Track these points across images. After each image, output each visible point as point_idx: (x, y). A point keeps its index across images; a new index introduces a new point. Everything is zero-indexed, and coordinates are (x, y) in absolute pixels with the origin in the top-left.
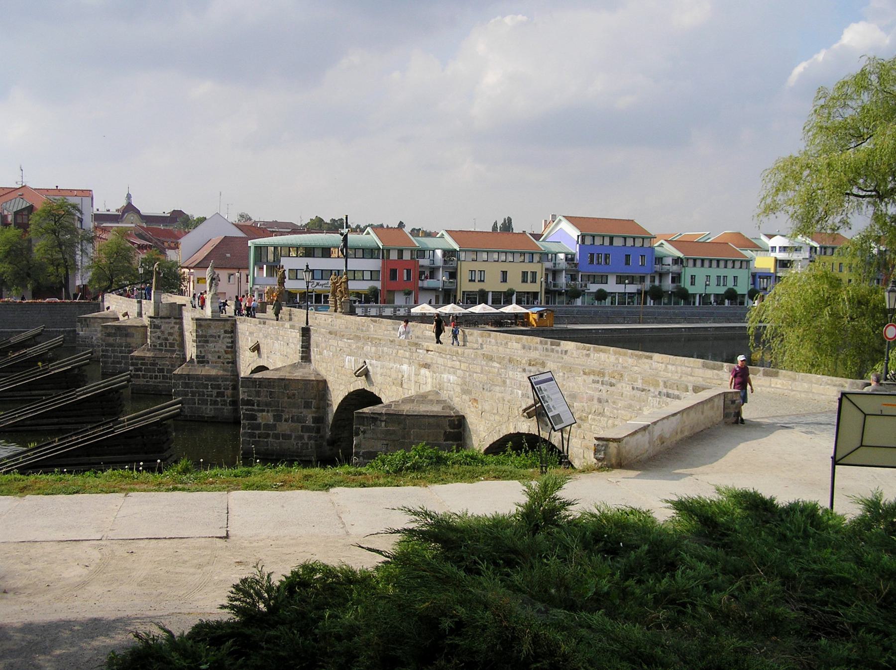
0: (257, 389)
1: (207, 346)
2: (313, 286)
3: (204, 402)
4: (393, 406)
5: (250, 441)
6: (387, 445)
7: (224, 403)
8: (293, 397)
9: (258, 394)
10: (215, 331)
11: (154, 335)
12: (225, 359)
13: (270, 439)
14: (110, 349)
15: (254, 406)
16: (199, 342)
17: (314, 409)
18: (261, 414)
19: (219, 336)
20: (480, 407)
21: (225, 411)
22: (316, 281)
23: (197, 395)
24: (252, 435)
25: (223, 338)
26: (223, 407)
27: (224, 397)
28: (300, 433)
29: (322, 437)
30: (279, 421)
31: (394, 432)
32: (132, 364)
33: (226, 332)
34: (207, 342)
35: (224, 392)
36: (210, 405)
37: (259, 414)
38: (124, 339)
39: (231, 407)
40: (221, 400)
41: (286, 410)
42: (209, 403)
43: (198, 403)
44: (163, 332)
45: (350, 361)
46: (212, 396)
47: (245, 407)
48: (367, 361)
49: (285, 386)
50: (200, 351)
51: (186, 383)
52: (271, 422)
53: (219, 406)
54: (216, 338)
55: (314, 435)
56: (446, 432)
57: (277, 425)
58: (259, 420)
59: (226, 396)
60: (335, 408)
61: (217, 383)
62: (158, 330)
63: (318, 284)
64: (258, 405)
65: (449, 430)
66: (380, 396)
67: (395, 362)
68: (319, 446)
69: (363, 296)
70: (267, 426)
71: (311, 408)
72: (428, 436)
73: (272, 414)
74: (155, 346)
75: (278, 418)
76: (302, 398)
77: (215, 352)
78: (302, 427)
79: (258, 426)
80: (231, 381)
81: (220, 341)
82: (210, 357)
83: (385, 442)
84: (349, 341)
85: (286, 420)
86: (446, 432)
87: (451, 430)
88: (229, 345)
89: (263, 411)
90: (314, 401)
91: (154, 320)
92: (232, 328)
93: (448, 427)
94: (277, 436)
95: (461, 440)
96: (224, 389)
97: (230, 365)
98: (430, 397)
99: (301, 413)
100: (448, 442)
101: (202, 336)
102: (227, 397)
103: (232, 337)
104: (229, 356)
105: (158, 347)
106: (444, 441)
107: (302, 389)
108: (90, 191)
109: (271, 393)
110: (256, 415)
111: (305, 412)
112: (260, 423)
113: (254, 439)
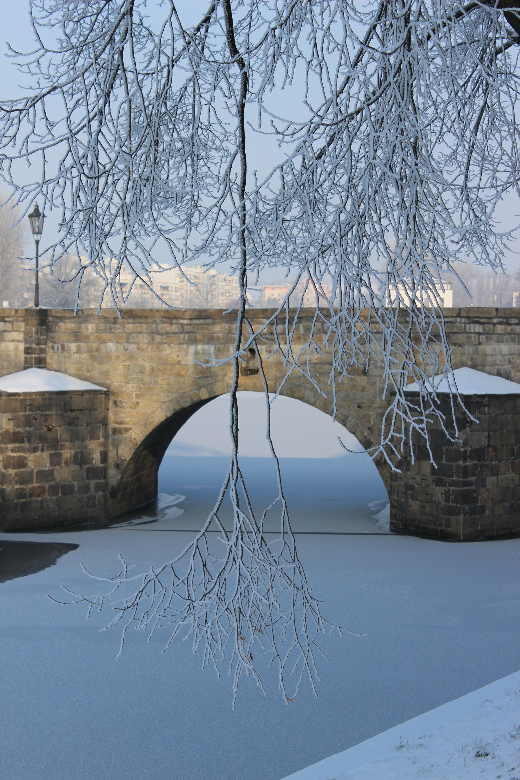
5: (17, 504)
13: (46, 496)
15: (23, 442)
18: (32, 455)
52: (48, 467)
57: (55, 472)
64: (29, 442)
113: (23, 500)
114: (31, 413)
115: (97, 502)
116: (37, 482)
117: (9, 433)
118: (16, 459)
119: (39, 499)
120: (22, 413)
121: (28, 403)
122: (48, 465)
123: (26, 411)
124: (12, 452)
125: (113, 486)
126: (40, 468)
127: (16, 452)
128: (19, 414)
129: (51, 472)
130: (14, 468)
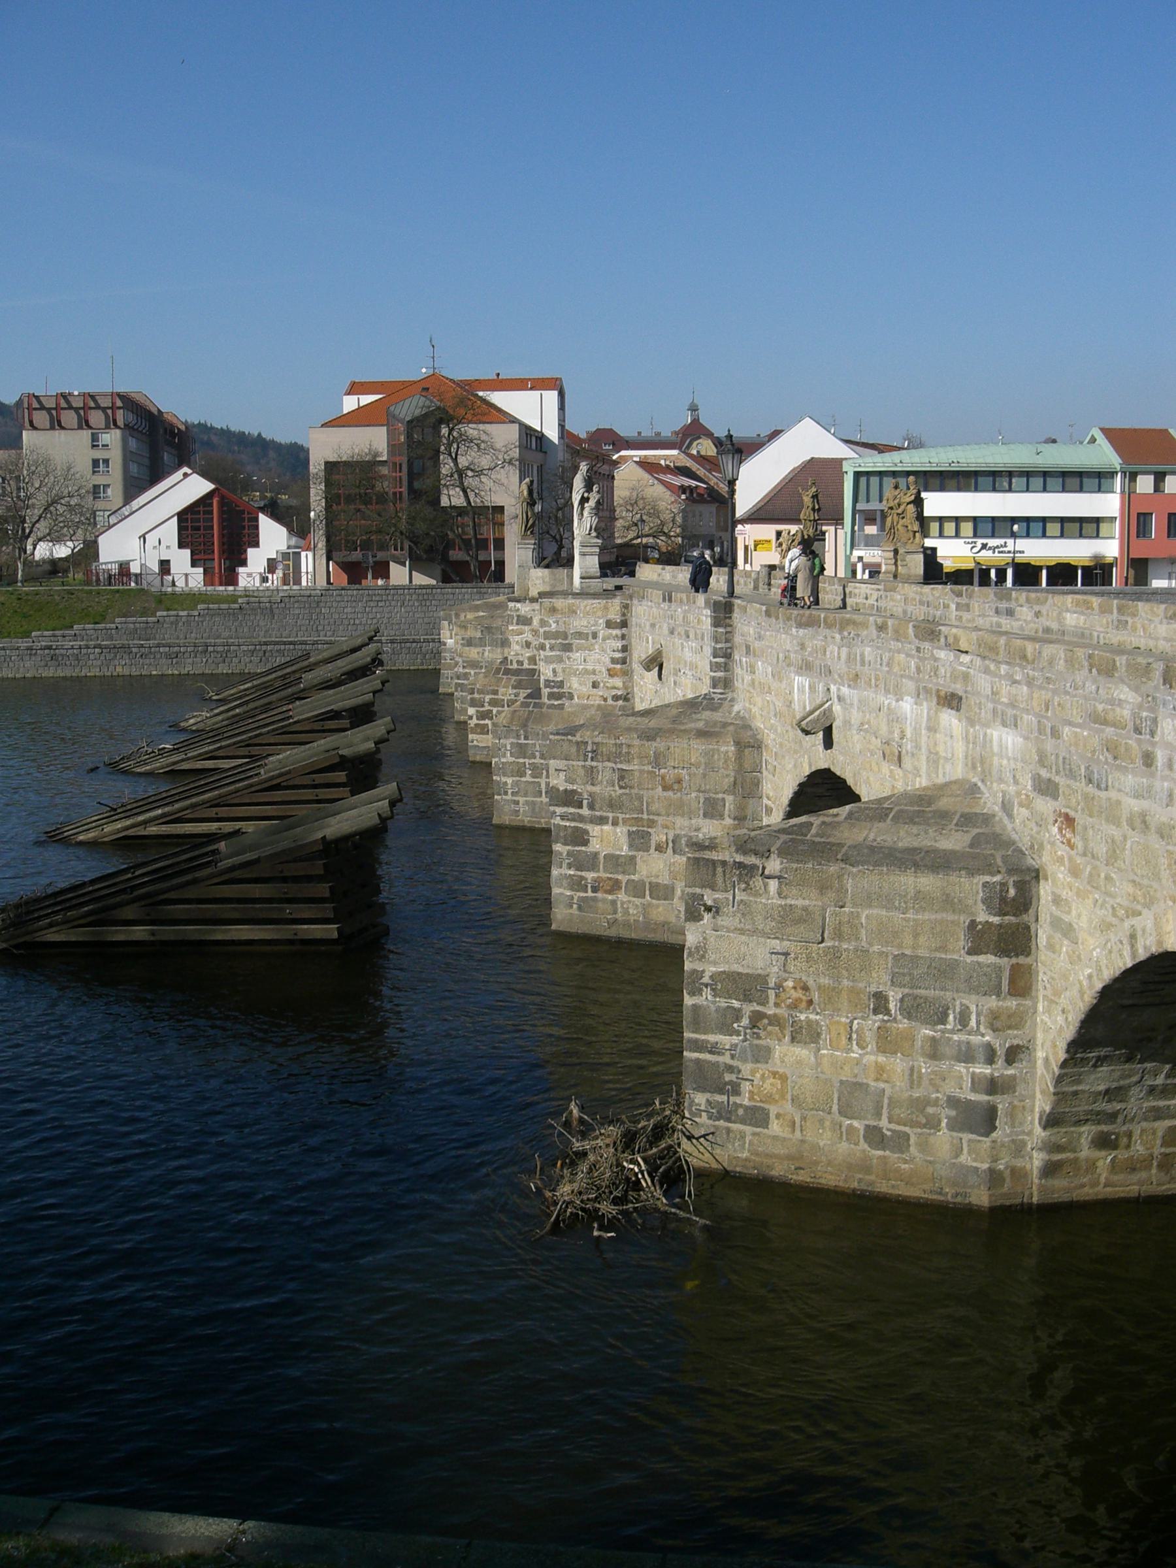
1: (569, 658)
2: (975, 550)
4: (813, 831)
5: (572, 897)
6: (786, 954)
8: (676, 786)
9: (591, 774)
10: (586, 624)
11: (517, 638)
13: (622, 896)
14: (472, 672)
15: (580, 806)
16: (552, 648)
17: (728, 821)
18: (597, 828)
19: (595, 635)
20: (1080, 845)
22: (980, 542)
24: (578, 884)
25: (604, 640)
31: (803, 917)
32: (473, 703)
33: (609, 624)
34: (567, 648)
37: (594, 830)
38: (499, 650)
41: (660, 820)
44: (535, 632)
45: (801, 690)
47: (559, 810)
48: (833, 688)
49: (657, 755)
50: (554, 671)
52: (625, 850)
54: (587, 639)
56: (973, 924)
57: (638, 860)
58: (595, 846)
62: (526, 628)
63: (984, 546)
64: (591, 807)
65: (983, 916)
67: (887, 691)
69: (1080, 572)
70: (614, 861)
71: (722, 817)
72: (916, 936)
73: (625, 829)
74: (520, 663)
75: (640, 840)
76: (699, 791)
77: (586, 672)
79: (591, 862)
81: (597, 647)
82: (575, 685)
83: (776, 944)
85: (659, 848)
86: (973, 924)
87: (996, 920)
88: (618, 655)
89: (602, 821)
90: (729, 799)
91: (518, 605)
92: (624, 615)
93: (981, 906)
94: (637, 889)
95: (1028, 954)
97: (620, 703)
98: (944, 803)
99: (698, 830)
100: (981, 958)
101: (556, 635)
103: (623, 637)
104: (618, 682)
105: (526, 666)
106: (969, 953)
107: (697, 765)
108: (557, 379)
109: (622, 775)
110: (586, 832)
112: (596, 855)
114: (594, 764)
116: (605, 871)
118: (570, 830)
119: (610, 897)
121: (589, 749)
123: (585, 760)
124: (563, 819)
126: (612, 851)
127: (568, 820)
128: (574, 763)
129: (632, 859)
130: (565, 844)
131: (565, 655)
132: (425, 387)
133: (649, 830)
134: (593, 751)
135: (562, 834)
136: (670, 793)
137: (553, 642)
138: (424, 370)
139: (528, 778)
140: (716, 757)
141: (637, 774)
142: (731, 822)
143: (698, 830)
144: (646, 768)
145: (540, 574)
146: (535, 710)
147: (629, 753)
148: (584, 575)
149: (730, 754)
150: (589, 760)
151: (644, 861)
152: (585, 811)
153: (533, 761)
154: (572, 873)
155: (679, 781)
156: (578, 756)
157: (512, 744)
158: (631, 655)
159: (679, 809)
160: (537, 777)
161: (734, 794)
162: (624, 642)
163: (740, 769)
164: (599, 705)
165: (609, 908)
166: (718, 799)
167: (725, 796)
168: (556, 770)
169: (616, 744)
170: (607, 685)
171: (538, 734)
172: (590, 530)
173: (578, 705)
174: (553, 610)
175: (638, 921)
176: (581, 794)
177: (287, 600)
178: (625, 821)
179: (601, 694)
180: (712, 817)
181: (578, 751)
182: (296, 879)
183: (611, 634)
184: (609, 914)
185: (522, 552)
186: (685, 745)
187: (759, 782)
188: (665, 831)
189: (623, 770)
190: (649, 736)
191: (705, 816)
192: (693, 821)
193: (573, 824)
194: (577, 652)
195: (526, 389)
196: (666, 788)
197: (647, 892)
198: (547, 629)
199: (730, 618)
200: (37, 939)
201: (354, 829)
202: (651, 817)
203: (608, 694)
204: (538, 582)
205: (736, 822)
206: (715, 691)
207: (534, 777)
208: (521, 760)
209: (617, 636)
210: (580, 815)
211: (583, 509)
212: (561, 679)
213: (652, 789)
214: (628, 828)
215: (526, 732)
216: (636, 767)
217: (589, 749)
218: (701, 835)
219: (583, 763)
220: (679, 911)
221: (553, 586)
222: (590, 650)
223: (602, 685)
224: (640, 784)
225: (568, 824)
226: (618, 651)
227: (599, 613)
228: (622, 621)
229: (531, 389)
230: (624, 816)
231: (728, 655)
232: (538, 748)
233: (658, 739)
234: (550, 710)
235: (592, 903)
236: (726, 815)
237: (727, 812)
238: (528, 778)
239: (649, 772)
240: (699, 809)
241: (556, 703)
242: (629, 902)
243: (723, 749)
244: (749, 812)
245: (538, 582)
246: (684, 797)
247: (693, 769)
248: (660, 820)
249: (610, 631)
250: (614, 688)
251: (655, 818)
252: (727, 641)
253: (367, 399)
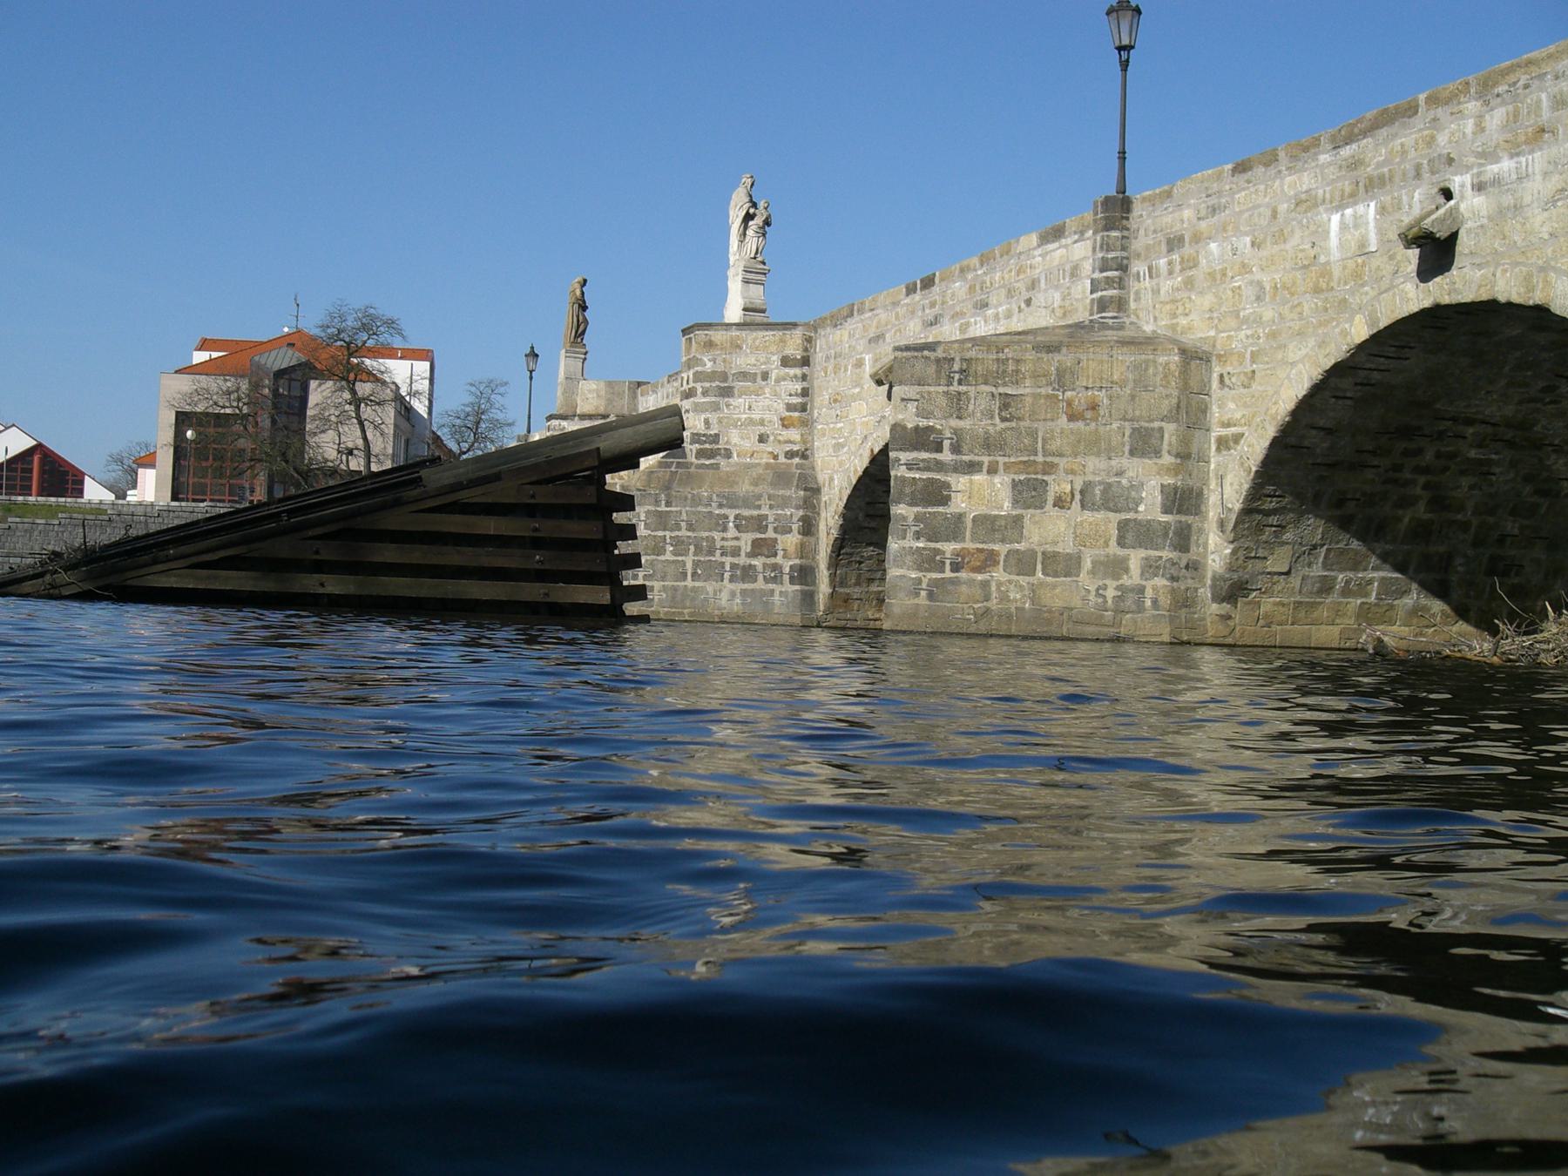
0: (955, 387)
3: (715, 572)
5: (919, 581)
7: (775, 574)
8: (1089, 415)
9: (958, 405)
10: (753, 361)
12: (779, 441)
13: (999, 574)
16: (705, 393)
17: (1167, 459)
19: (765, 376)
21: (777, 597)
23: (692, 547)
24: (930, 561)
25: (778, 381)
26: (771, 586)
27: (775, 555)
28: (1114, 549)
29: (1194, 567)
30: (1036, 508)
33: (786, 362)
34: (727, 392)
35: (776, 539)
36: (731, 581)
39: (797, 587)
40: (765, 565)
41: (1063, 463)
42: (727, 575)
43: (694, 574)
46: (736, 552)
47: (905, 456)
48: (1458, 182)
49: (1061, 374)
50: (707, 422)
51: (660, 514)
52: (1006, 507)
53: (760, 584)
54: (754, 381)
55: (1167, 554)
57: (1027, 521)
59: (781, 553)
60: (1255, 446)
61: (755, 513)
64: (956, 449)
66: (1537, 298)
68: (1184, 601)
70: (988, 525)
71: (1157, 453)
73: (1007, 479)
75: (1030, 493)
76: (1124, 419)
77: (751, 422)
78: (1123, 526)
79: (953, 530)
80: (798, 508)
81: (767, 390)
84: (1346, 151)
85: (1060, 503)
88: (797, 400)
89: (972, 468)
90: (1170, 428)
92: (806, 350)
94: (1023, 562)
96: (776, 530)
97: (797, 460)
99: (1120, 473)
101: (711, 376)
102: (784, 557)
103: (804, 377)
104: (794, 434)
107: (1122, 384)
108: (428, 351)
109: (1006, 402)
110: (947, 486)
111: (1136, 468)
112: (960, 517)
114: (963, 388)
115: (1148, 603)
117: (904, 428)
118: (920, 484)
119: (980, 577)
120: (941, 389)
121: (956, 367)
122: (1007, 505)
123: (950, 384)
125: (1214, 572)
127: (918, 469)
128: (932, 389)
129: (1017, 521)
130: (911, 505)
131: (722, 401)
132: (289, 342)
133: (1045, 478)
134: (962, 371)
135: (908, 490)
136: (1080, 425)
137: (707, 385)
138: (286, 330)
139: (668, 556)
140: (1151, 371)
141: (1029, 400)
142: (1173, 460)
143: (1120, 473)
144: (1043, 391)
145: (595, 387)
146: (680, 470)
147: (1017, 371)
148: (750, 306)
149: (1173, 367)
150: (955, 383)
151: (1036, 523)
152: (946, 456)
153: (677, 533)
154: (921, 545)
155: (1094, 407)
156: (939, 378)
157: (648, 512)
158: (812, 401)
159: (1094, 445)
160: (682, 555)
161: (1177, 421)
162: (805, 384)
163: (1185, 388)
164: (768, 466)
165: (978, 592)
166: (1153, 429)
167: (1163, 423)
168: (903, 400)
169: (998, 360)
170: (780, 438)
171: (686, 498)
172: (757, 253)
173: (737, 464)
174: (710, 345)
175: (1023, 609)
176: (940, 432)
177: (165, 514)
178: (1007, 467)
179: (770, 449)
180: (1143, 455)
181: (938, 372)
182: (549, 511)
183: (788, 374)
184: (978, 602)
185: (571, 361)
186: (1105, 357)
187: (1206, 407)
188: (1070, 477)
189: (1006, 394)
190: (1052, 348)
191: (1132, 453)
192: (1113, 463)
193: (925, 475)
194: (740, 397)
195: (397, 358)
196: (1072, 418)
197: (1039, 567)
198: (699, 369)
199: (1127, 219)
200: (129, 582)
201: (639, 444)
202: (1049, 459)
203: (780, 450)
204: (590, 396)
205: (1179, 461)
206: (1104, 315)
207: (675, 555)
208: (660, 533)
209: (796, 376)
210: (938, 462)
211: (746, 228)
212: (716, 432)
213: (1052, 420)
214: (1012, 476)
215: (668, 496)
216: (1028, 391)
217: (956, 367)
218: (1124, 482)
219: (945, 389)
220: (1088, 591)
221: (610, 401)
222: (758, 395)
223: (772, 438)
224: (1033, 413)
225: (917, 476)
226: (796, 395)
227: (773, 348)
228: (803, 357)
229: (401, 358)
230: (1006, 459)
231: (1123, 268)
232: (684, 517)
233: (1064, 350)
234: (700, 471)
235: (950, 587)
236: (1164, 453)
237: (1165, 447)
238: (668, 556)
239: (1048, 397)
240: (1123, 444)
241: (707, 462)
242: (1010, 582)
243: (1162, 359)
244: (1194, 450)
245: (590, 396)
246: (1101, 429)
247: (1116, 389)
248: (1063, 463)
249: (787, 370)
250: (791, 442)
251: (1056, 460)
252: (1124, 249)
253: (215, 355)
